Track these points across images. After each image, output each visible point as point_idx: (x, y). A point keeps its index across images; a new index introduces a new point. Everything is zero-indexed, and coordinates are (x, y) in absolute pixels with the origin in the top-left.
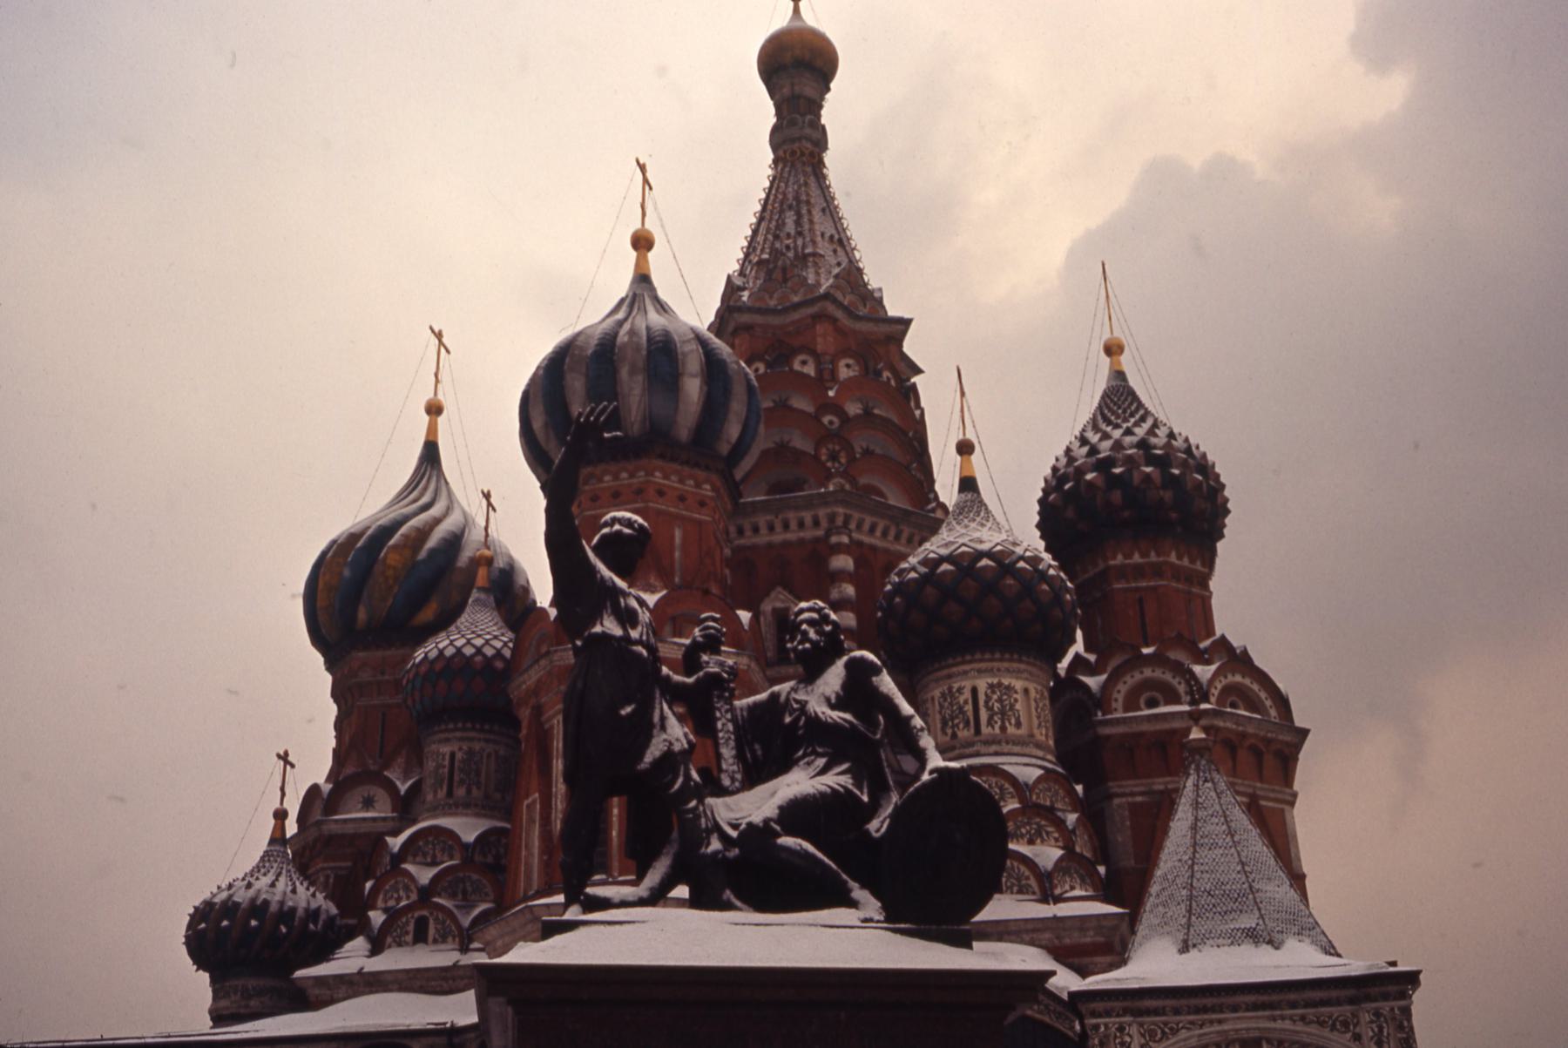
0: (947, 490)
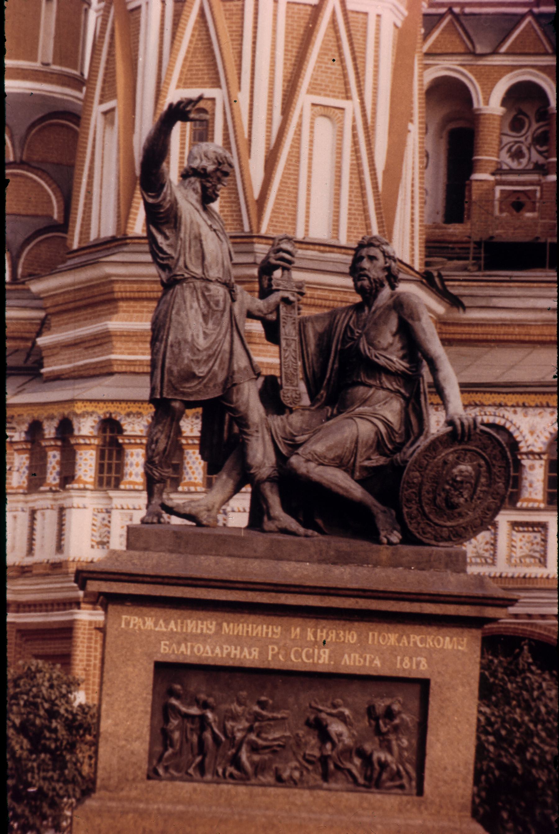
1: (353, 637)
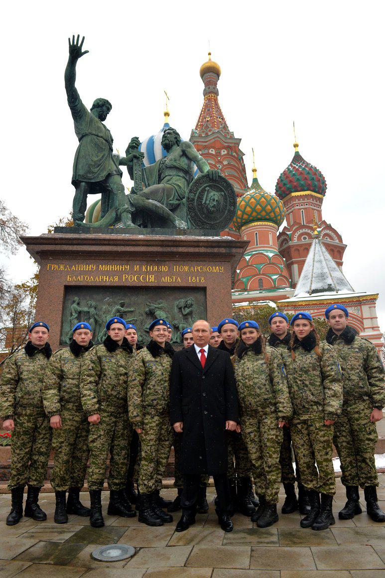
0: (250, 183)
1: (166, 269)
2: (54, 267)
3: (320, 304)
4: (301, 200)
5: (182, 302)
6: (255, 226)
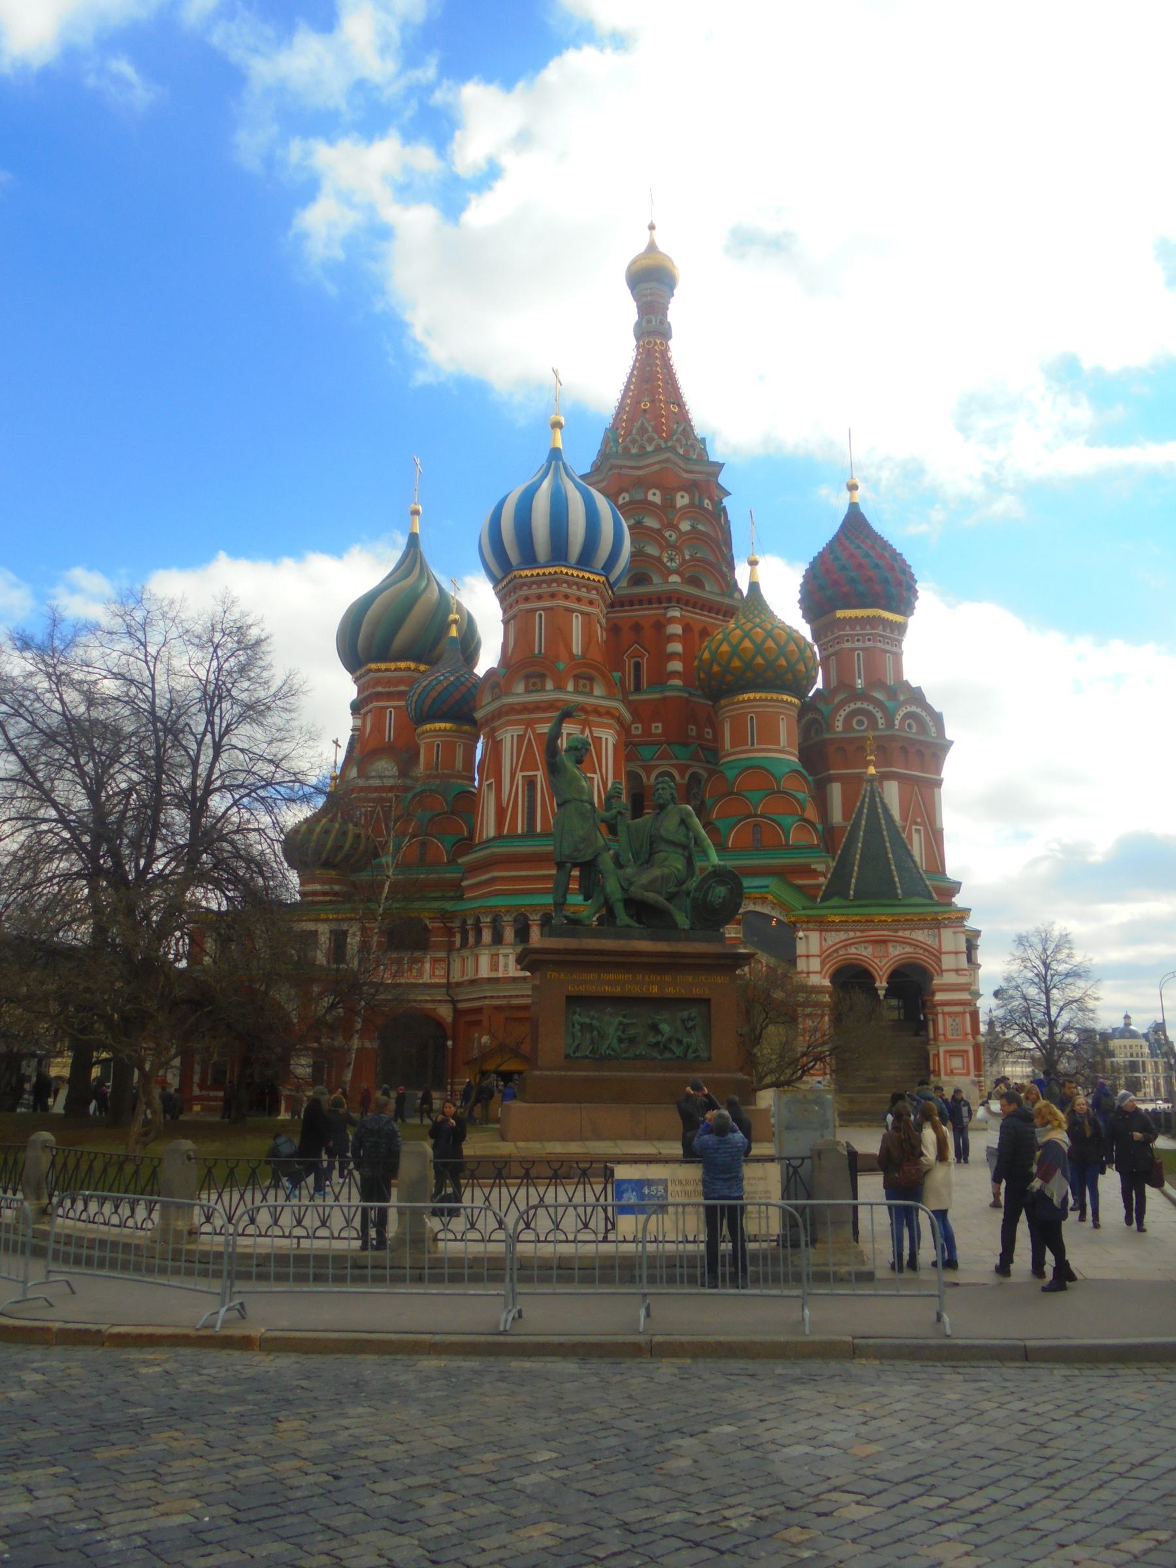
2: (554, 975)
3: (867, 921)
4: (858, 628)
5: (686, 1014)
6: (749, 700)
